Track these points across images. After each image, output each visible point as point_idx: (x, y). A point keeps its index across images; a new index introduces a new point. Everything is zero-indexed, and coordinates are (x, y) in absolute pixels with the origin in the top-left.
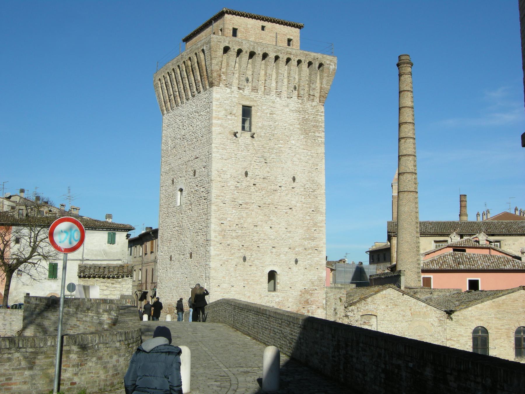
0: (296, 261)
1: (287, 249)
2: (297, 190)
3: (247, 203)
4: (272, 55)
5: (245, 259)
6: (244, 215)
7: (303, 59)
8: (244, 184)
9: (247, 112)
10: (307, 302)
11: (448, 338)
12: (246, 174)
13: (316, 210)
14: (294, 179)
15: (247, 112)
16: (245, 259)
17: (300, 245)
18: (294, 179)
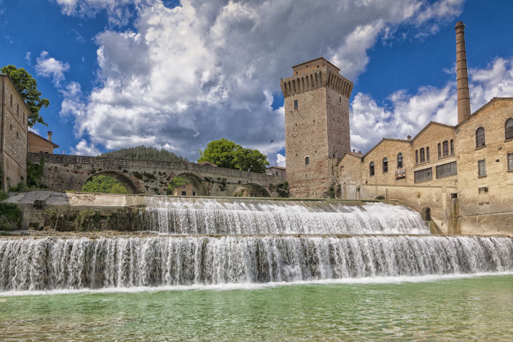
0: (316, 152)
1: (312, 148)
2: (315, 125)
3: (297, 135)
4: (300, 78)
5: (297, 155)
6: (296, 139)
7: (312, 73)
8: (296, 128)
9: (296, 102)
10: (320, 166)
11: (363, 169)
12: (296, 125)
13: (324, 130)
14: (314, 121)
15: (296, 102)
16: (297, 155)
17: (317, 145)
18: (314, 121)
